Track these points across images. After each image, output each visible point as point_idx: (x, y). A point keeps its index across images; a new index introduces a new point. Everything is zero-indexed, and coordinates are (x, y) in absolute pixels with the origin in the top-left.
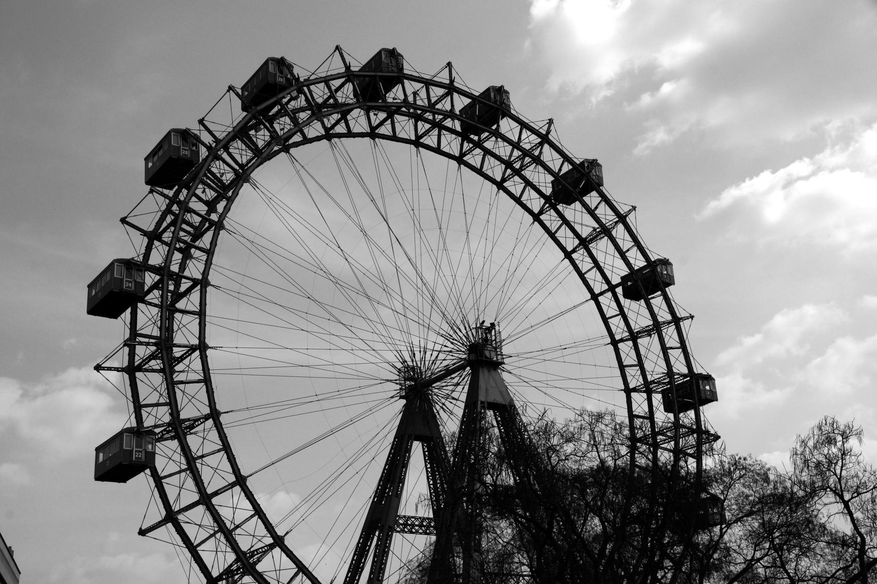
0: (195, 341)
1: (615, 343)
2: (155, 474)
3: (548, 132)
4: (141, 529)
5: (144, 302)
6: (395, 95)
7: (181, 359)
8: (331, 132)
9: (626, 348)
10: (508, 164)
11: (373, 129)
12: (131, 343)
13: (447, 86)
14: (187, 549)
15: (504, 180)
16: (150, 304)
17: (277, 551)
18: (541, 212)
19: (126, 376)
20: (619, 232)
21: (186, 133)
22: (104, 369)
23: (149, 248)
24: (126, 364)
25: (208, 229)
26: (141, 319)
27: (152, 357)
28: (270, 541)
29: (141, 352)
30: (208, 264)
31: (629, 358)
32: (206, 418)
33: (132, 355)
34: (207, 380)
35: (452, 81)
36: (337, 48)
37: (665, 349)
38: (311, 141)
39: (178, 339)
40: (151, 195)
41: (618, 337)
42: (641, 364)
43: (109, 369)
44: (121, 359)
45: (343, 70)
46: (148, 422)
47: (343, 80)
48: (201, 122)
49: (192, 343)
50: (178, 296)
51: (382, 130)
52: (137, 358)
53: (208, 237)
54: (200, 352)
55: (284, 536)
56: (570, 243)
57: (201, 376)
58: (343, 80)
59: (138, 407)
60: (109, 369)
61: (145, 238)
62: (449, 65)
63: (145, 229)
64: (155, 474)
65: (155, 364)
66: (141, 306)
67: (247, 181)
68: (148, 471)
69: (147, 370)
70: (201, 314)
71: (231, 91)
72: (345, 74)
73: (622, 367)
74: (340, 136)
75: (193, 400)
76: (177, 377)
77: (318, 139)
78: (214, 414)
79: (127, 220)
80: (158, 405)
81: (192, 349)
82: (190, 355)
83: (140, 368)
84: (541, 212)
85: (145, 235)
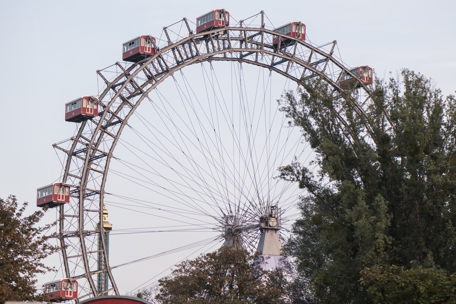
0: (107, 151)
2: (61, 211)
4: (44, 235)
5: (91, 119)
6: (290, 49)
7: (98, 157)
8: (244, 58)
11: (273, 64)
12: (75, 140)
13: (327, 55)
14: (62, 257)
16: (94, 122)
19: (67, 156)
21: (148, 38)
22: (57, 147)
23: (106, 92)
24: (69, 149)
25: (138, 94)
26: (86, 129)
27: (83, 151)
29: (79, 146)
30: (131, 113)
32: (97, 193)
33: (74, 146)
34: (104, 174)
36: (262, 12)
38: (228, 59)
39: (100, 147)
40: (115, 65)
43: (60, 148)
44: (68, 146)
45: (259, 27)
46: (68, 182)
47: (258, 32)
48: (165, 29)
49: (105, 151)
50: (110, 124)
51: (278, 67)
52: (75, 149)
53: (138, 97)
54: (108, 158)
57: (102, 170)
58: (258, 32)
59: (67, 174)
60: (60, 148)
61: (106, 85)
62: (335, 42)
63: (108, 81)
64: (61, 211)
65: (83, 155)
66: (89, 121)
67: (172, 75)
68: (58, 208)
69: (79, 157)
70: (116, 138)
71: (184, 21)
72: (259, 30)
74: (249, 62)
75: (94, 180)
76: (93, 166)
77: (233, 59)
78: (101, 193)
79: (101, 72)
80: (76, 177)
81: (104, 155)
82: (102, 157)
83: (75, 154)
85: (107, 83)
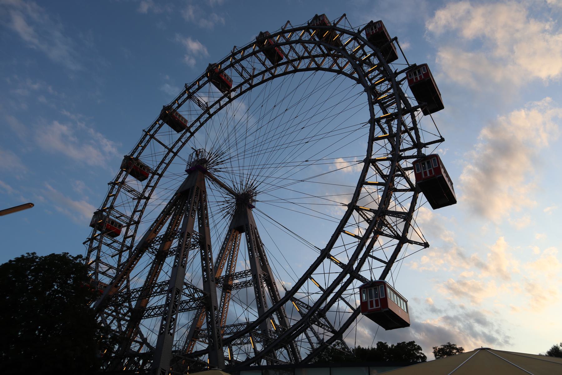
1: (211, 116)
3: (112, 183)
9: (212, 111)
10: (139, 199)
15: (145, 198)
17: (332, 253)
18: (158, 174)
20: (151, 133)
28: (326, 261)
31: (217, 106)
35: (89, 239)
37: (200, 87)
41: (208, 116)
42: (218, 101)
55: (320, 250)
56: (171, 154)
62: (84, 243)
73: (221, 108)
84: (158, 174)
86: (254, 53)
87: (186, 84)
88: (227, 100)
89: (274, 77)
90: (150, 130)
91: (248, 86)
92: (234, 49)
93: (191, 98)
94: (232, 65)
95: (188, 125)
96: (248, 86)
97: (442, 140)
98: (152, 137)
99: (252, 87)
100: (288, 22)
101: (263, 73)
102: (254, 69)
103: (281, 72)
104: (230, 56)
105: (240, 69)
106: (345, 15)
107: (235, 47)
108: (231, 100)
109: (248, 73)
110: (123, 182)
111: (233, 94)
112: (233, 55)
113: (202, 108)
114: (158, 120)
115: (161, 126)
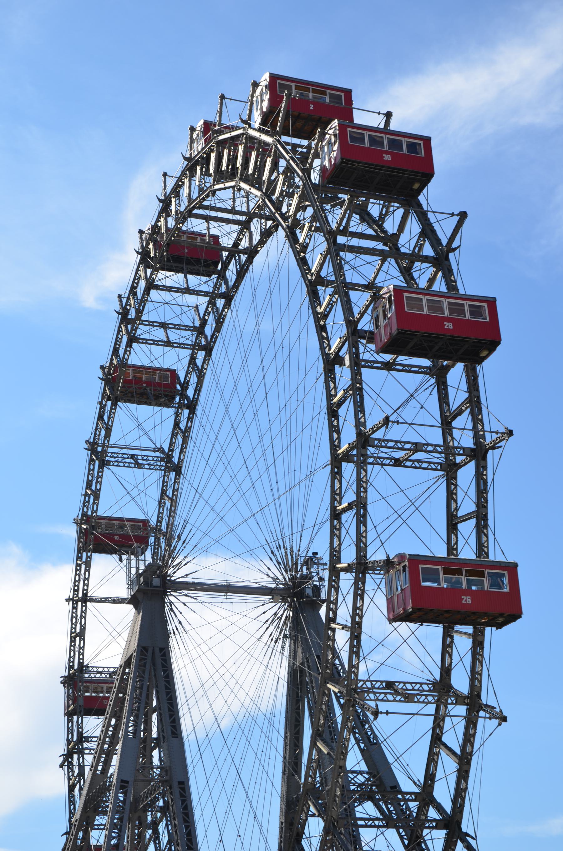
1: (178, 469)
86: (151, 285)
87: (87, 442)
88: (186, 412)
89: (229, 298)
90: (76, 591)
91: (203, 353)
92: (121, 301)
93: (108, 463)
94: (133, 339)
95: (153, 522)
96: (203, 353)
97: (463, 216)
98: (85, 599)
99: (208, 350)
100: (165, 175)
101: (212, 303)
102: (197, 307)
103: (234, 278)
104: (121, 322)
105: (159, 334)
106: (222, 97)
107: (120, 296)
108: (192, 406)
109: (187, 328)
110: (82, 738)
111: (190, 392)
112: (124, 314)
113: (147, 467)
114: (79, 558)
115: (88, 564)
